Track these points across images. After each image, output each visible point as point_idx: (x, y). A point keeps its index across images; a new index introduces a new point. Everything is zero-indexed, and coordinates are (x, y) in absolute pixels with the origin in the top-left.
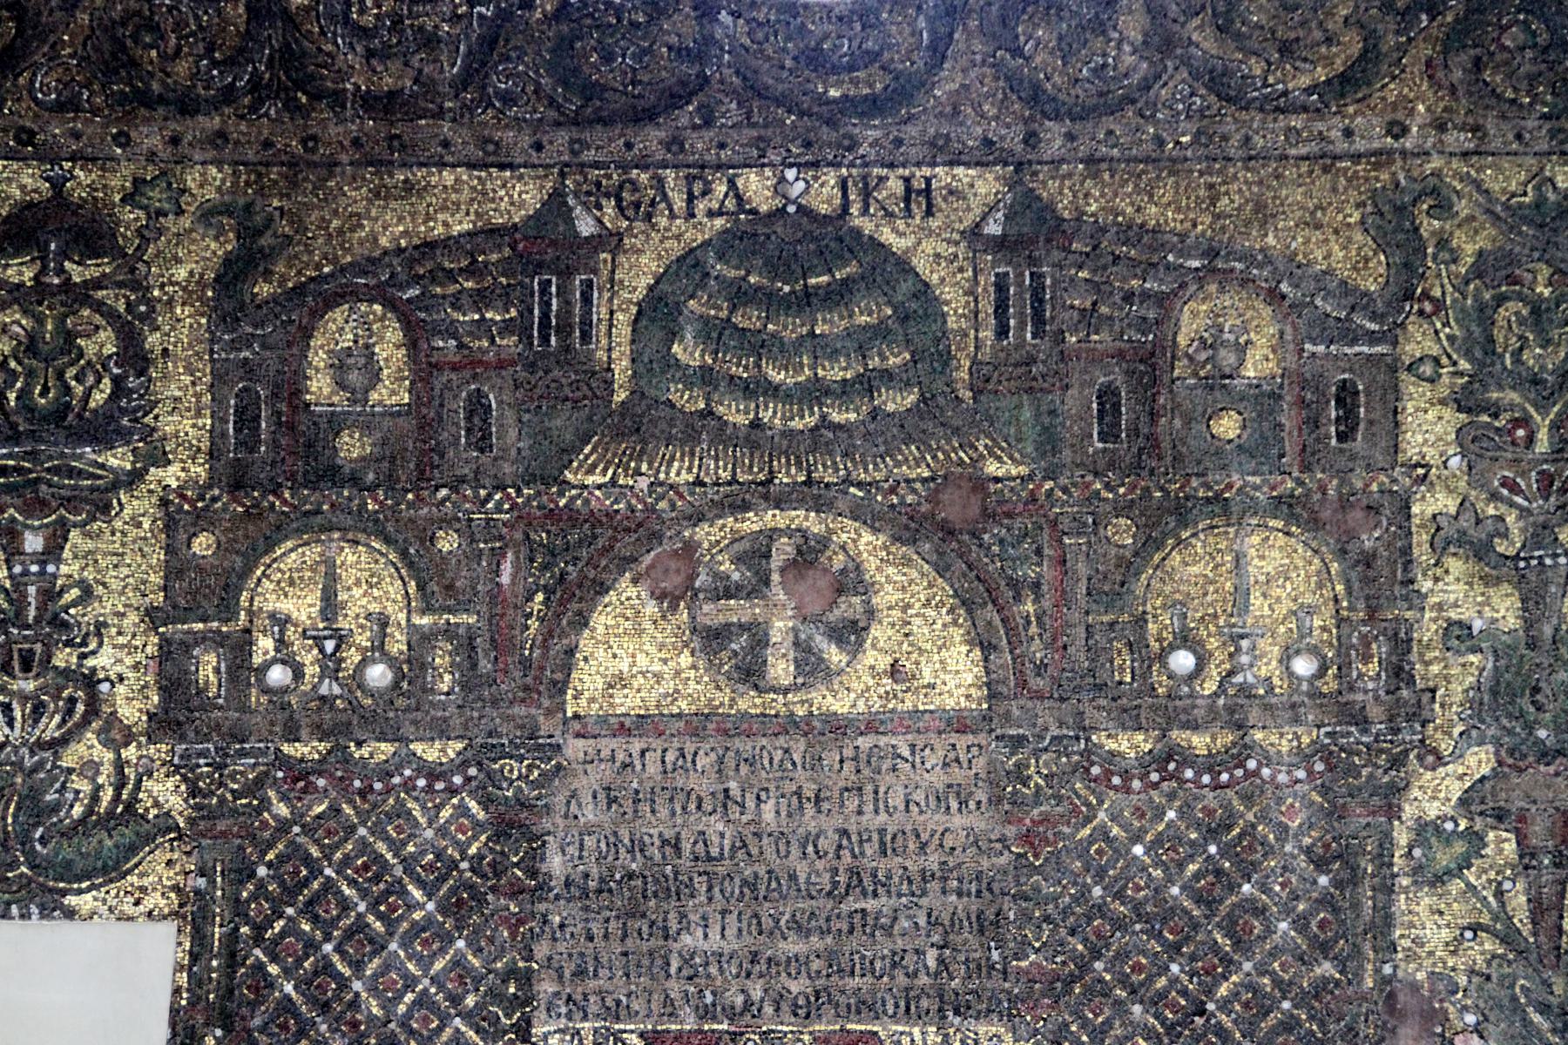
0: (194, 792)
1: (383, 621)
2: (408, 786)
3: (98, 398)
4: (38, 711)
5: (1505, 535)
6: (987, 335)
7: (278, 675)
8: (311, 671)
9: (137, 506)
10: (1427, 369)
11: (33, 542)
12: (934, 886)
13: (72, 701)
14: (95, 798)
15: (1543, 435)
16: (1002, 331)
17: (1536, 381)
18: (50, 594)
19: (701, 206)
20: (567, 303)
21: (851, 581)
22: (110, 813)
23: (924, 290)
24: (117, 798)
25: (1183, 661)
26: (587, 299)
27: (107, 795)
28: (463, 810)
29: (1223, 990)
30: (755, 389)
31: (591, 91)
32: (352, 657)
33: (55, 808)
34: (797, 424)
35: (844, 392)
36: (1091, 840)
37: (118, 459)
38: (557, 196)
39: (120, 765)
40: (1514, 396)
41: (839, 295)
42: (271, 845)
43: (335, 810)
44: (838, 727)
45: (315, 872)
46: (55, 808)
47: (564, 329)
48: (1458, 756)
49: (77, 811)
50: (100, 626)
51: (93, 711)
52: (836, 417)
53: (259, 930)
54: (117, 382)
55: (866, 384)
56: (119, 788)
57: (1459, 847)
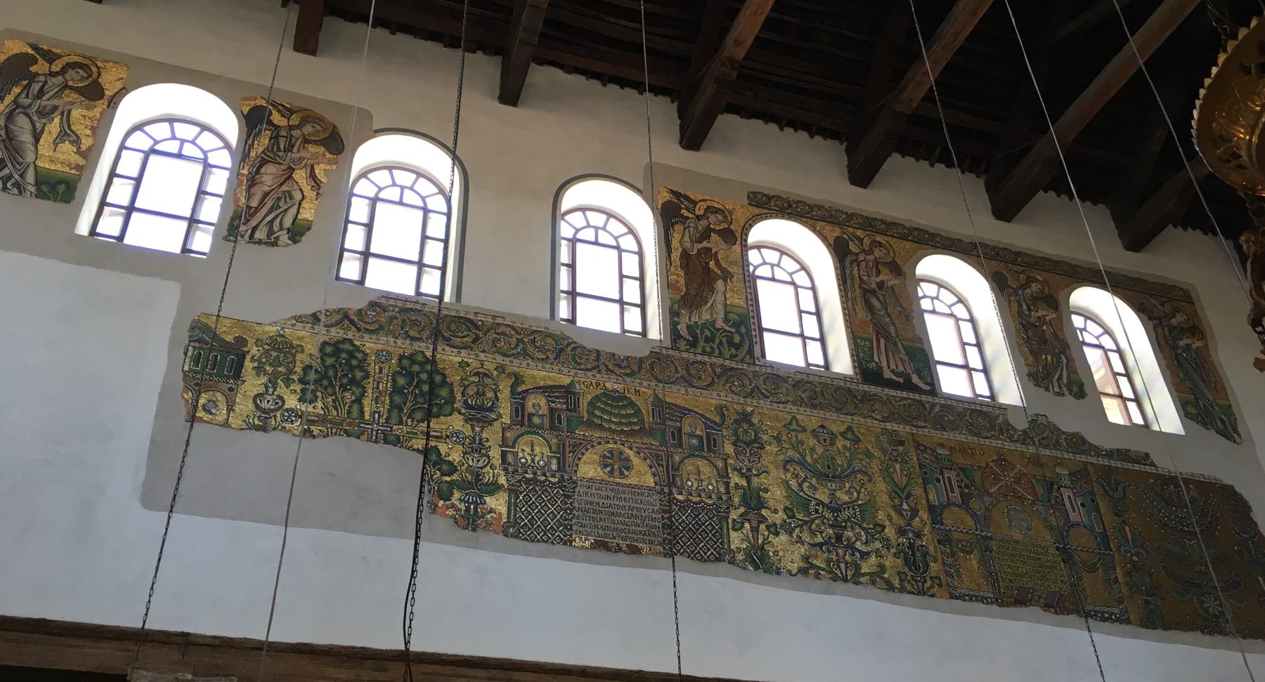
0: (508, 480)
1: (543, 454)
2: (548, 485)
3: (489, 405)
4: (478, 461)
5: (743, 469)
6: (651, 419)
7: (523, 460)
8: (530, 461)
9: (497, 425)
10: (727, 437)
11: (477, 429)
12: (647, 519)
13: (485, 460)
14: (489, 479)
15: (748, 452)
16: (653, 418)
17: (747, 443)
18: (481, 439)
19: (599, 388)
20: (575, 400)
21: (628, 460)
22: (492, 482)
23: (639, 409)
24: (493, 480)
25: (690, 483)
26: (579, 401)
27: (491, 479)
28: (558, 492)
29: (700, 546)
30: (610, 421)
31: (580, 364)
32: (537, 459)
33: (482, 480)
34: (617, 429)
35: (626, 424)
36: (675, 514)
37: (493, 416)
38: (573, 381)
39: (494, 473)
40: (742, 445)
41: (624, 407)
42: (522, 492)
43: (534, 488)
44: (629, 486)
45: (531, 499)
46: (482, 480)
47: (575, 405)
48: (738, 508)
49: (486, 481)
50: (490, 446)
51: (489, 462)
52: (624, 429)
53: (521, 509)
54: (493, 402)
55: (630, 423)
56: (494, 477)
57: (740, 525)
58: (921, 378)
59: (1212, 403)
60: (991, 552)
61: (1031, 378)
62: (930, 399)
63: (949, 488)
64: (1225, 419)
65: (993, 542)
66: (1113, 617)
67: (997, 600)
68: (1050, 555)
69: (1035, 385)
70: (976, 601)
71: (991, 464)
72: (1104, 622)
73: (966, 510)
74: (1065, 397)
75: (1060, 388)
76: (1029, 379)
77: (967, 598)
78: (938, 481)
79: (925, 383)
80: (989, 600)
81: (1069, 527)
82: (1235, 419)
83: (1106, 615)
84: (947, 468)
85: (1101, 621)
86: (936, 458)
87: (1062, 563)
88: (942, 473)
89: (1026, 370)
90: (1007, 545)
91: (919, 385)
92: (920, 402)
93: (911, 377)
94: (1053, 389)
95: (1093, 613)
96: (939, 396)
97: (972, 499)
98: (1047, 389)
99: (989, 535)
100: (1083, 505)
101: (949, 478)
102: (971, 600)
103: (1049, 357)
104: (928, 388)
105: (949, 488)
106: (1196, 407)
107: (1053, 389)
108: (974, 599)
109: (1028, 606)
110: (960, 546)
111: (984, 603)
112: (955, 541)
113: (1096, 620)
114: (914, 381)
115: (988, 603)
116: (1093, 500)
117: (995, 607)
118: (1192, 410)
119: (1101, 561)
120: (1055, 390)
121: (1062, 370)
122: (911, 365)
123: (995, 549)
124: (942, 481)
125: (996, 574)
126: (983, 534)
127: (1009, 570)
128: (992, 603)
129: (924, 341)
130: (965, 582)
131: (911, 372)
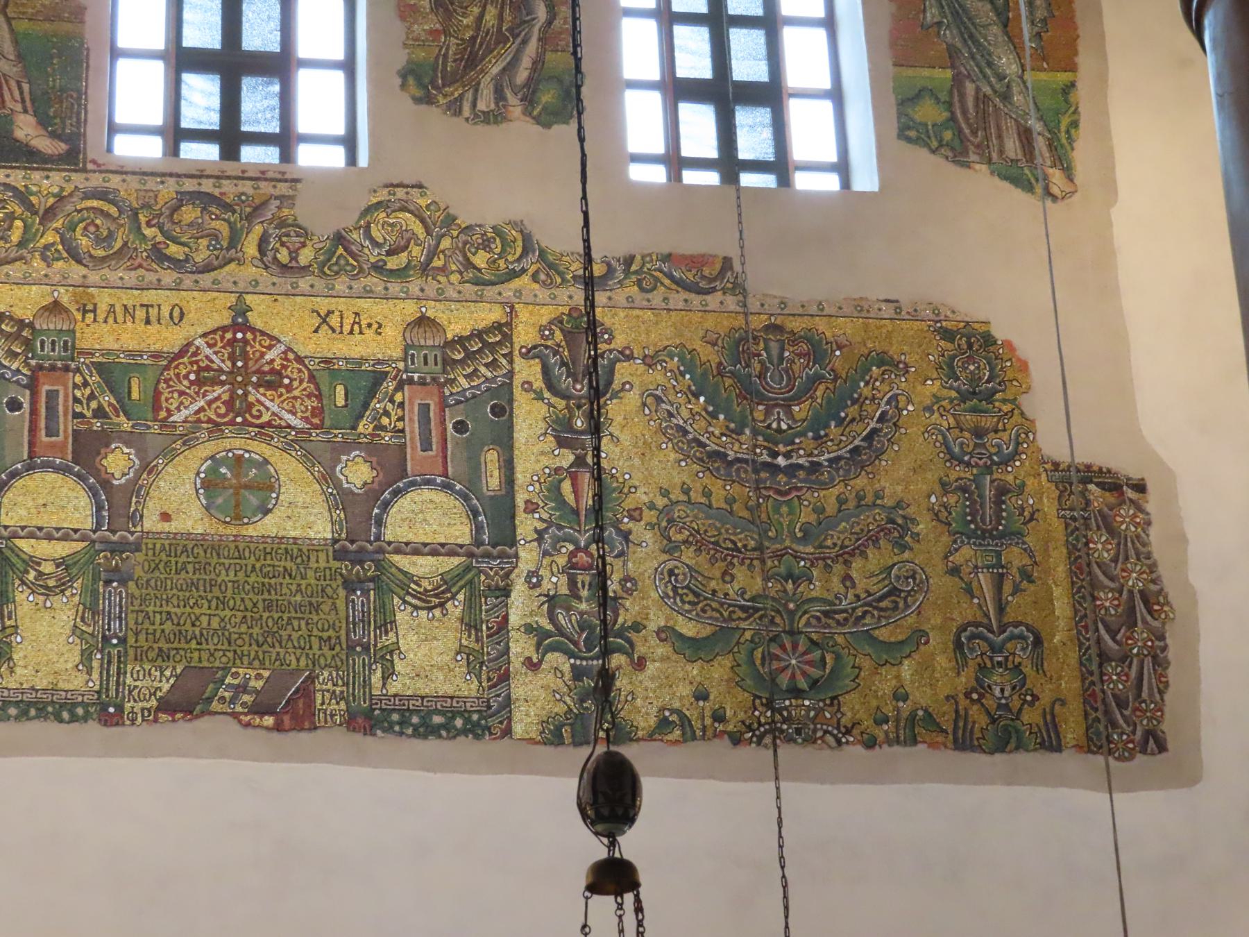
58: (43, 121)
59: (1008, 86)
60: (123, 582)
61: (411, 81)
62: (57, 177)
63: (42, 424)
64: (1037, 126)
65: (140, 556)
66: (459, 723)
67: (104, 707)
68: (310, 574)
69: (418, 101)
70: (37, 717)
71: (199, 342)
72: (425, 737)
73: (78, 476)
74: (504, 125)
75: (499, 95)
76: (403, 86)
77: (13, 711)
78: (14, 405)
79: (54, 135)
80: (80, 711)
81: (397, 493)
82: (1075, 124)
83: (437, 719)
84: (53, 368)
85: (416, 734)
86: (28, 344)
87: (342, 593)
88: (33, 386)
89: (400, 59)
90: (183, 558)
91: (35, 143)
92: (22, 197)
93: (11, 122)
94: (474, 105)
95: (395, 717)
96: (90, 166)
97: (107, 446)
98: (455, 108)
99: (131, 538)
100: (460, 427)
101: (52, 395)
102: (23, 715)
103: (491, 14)
104: (62, 147)
105: (42, 424)
106: (949, 105)
107: (474, 105)
108: (33, 712)
109: (197, 717)
110: (32, 575)
111: (61, 721)
112: (20, 565)
113: (401, 733)
114: (19, 134)
115: (74, 719)
116: (498, 411)
117: (93, 729)
118: (929, 112)
119: (469, 576)
120: (481, 106)
121: (525, 42)
122: (26, 87)
123: (138, 572)
124: (26, 406)
125: (123, 641)
126: (115, 538)
127: (168, 626)
128: (85, 718)
129: (88, 18)
130: (18, 671)
131: (19, 107)
